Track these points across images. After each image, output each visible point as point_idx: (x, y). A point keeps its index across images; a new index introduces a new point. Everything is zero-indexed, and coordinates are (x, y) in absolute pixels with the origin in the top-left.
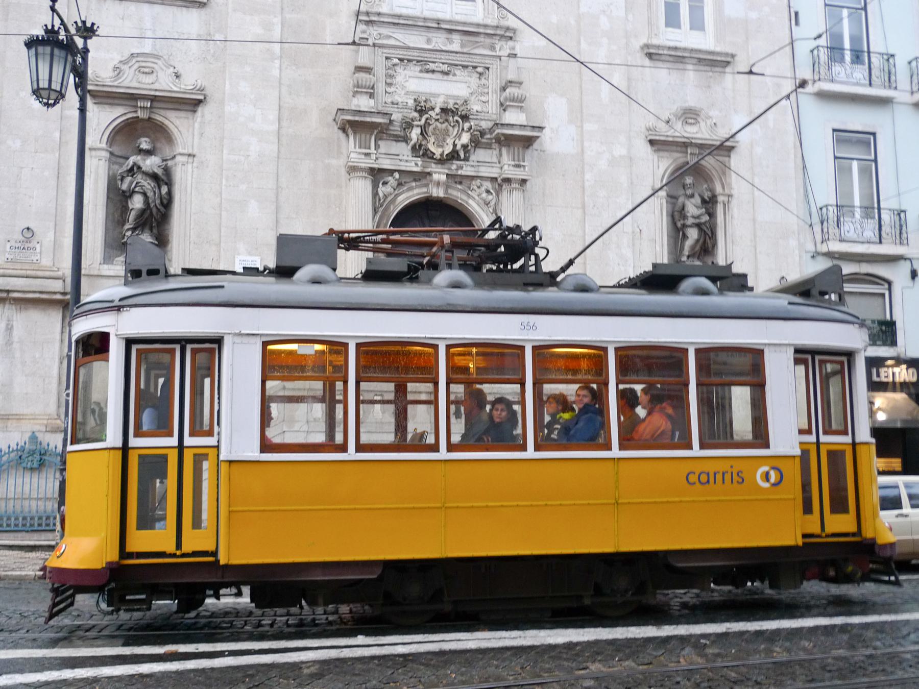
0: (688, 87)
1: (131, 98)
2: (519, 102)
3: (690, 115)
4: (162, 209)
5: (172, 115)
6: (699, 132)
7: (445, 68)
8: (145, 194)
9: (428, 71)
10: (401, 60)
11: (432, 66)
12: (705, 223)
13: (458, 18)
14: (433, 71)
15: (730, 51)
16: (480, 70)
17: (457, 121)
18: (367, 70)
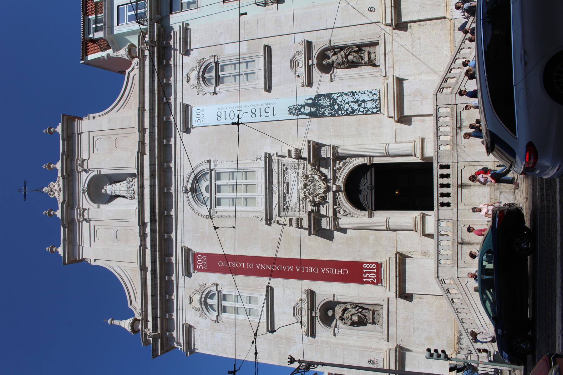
0: (280, 65)
1: (312, 321)
2: (298, 151)
3: (294, 63)
4: (358, 308)
5: (317, 303)
6: (302, 59)
7: (285, 185)
8: (351, 315)
9: (288, 193)
10: (284, 205)
11: (285, 191)
12: (345, 54)
13: (263, 180)
14: (288, 189)
15: (263, 48)
16: (284, 169)
17: (309, 181)
18: (291, 220)
